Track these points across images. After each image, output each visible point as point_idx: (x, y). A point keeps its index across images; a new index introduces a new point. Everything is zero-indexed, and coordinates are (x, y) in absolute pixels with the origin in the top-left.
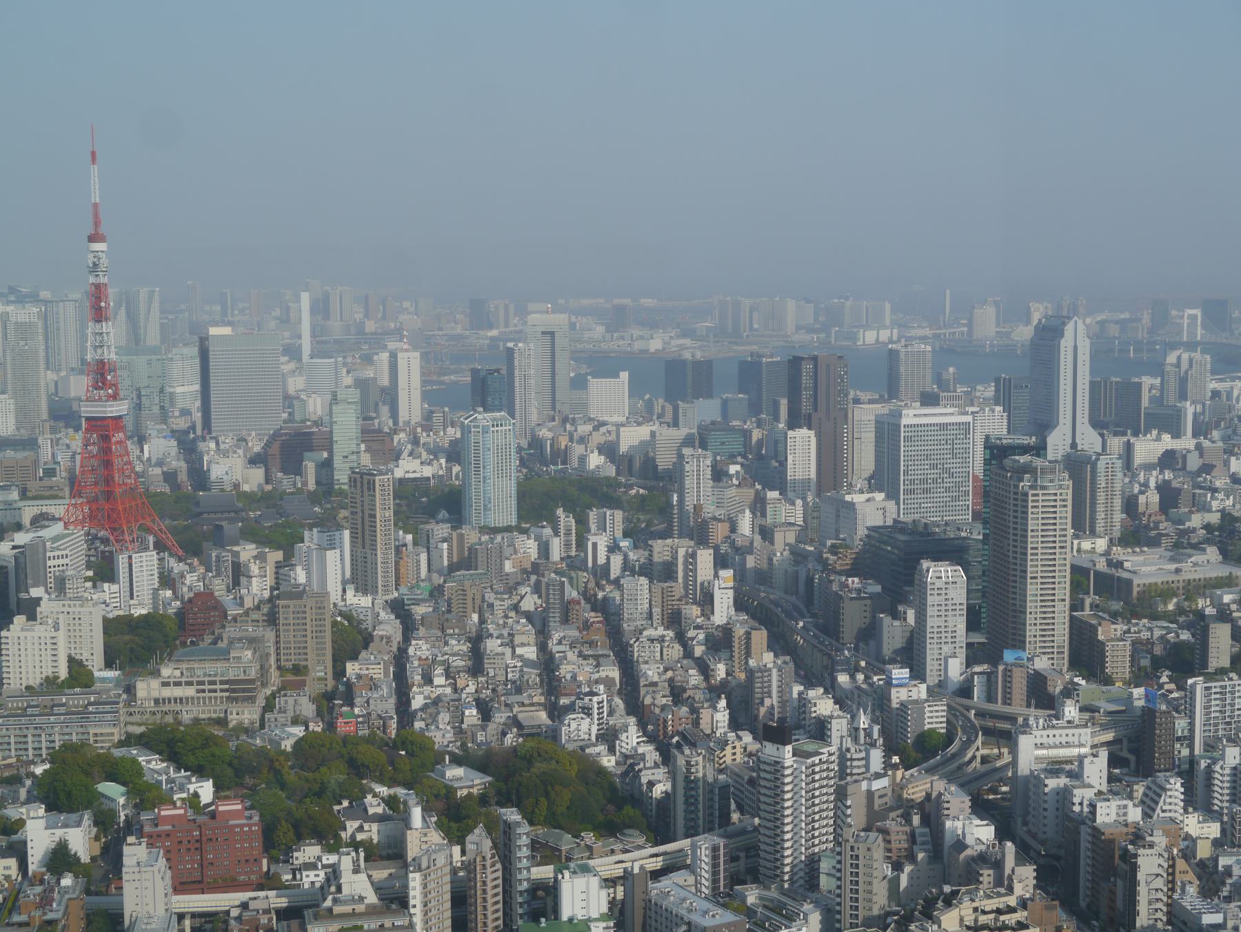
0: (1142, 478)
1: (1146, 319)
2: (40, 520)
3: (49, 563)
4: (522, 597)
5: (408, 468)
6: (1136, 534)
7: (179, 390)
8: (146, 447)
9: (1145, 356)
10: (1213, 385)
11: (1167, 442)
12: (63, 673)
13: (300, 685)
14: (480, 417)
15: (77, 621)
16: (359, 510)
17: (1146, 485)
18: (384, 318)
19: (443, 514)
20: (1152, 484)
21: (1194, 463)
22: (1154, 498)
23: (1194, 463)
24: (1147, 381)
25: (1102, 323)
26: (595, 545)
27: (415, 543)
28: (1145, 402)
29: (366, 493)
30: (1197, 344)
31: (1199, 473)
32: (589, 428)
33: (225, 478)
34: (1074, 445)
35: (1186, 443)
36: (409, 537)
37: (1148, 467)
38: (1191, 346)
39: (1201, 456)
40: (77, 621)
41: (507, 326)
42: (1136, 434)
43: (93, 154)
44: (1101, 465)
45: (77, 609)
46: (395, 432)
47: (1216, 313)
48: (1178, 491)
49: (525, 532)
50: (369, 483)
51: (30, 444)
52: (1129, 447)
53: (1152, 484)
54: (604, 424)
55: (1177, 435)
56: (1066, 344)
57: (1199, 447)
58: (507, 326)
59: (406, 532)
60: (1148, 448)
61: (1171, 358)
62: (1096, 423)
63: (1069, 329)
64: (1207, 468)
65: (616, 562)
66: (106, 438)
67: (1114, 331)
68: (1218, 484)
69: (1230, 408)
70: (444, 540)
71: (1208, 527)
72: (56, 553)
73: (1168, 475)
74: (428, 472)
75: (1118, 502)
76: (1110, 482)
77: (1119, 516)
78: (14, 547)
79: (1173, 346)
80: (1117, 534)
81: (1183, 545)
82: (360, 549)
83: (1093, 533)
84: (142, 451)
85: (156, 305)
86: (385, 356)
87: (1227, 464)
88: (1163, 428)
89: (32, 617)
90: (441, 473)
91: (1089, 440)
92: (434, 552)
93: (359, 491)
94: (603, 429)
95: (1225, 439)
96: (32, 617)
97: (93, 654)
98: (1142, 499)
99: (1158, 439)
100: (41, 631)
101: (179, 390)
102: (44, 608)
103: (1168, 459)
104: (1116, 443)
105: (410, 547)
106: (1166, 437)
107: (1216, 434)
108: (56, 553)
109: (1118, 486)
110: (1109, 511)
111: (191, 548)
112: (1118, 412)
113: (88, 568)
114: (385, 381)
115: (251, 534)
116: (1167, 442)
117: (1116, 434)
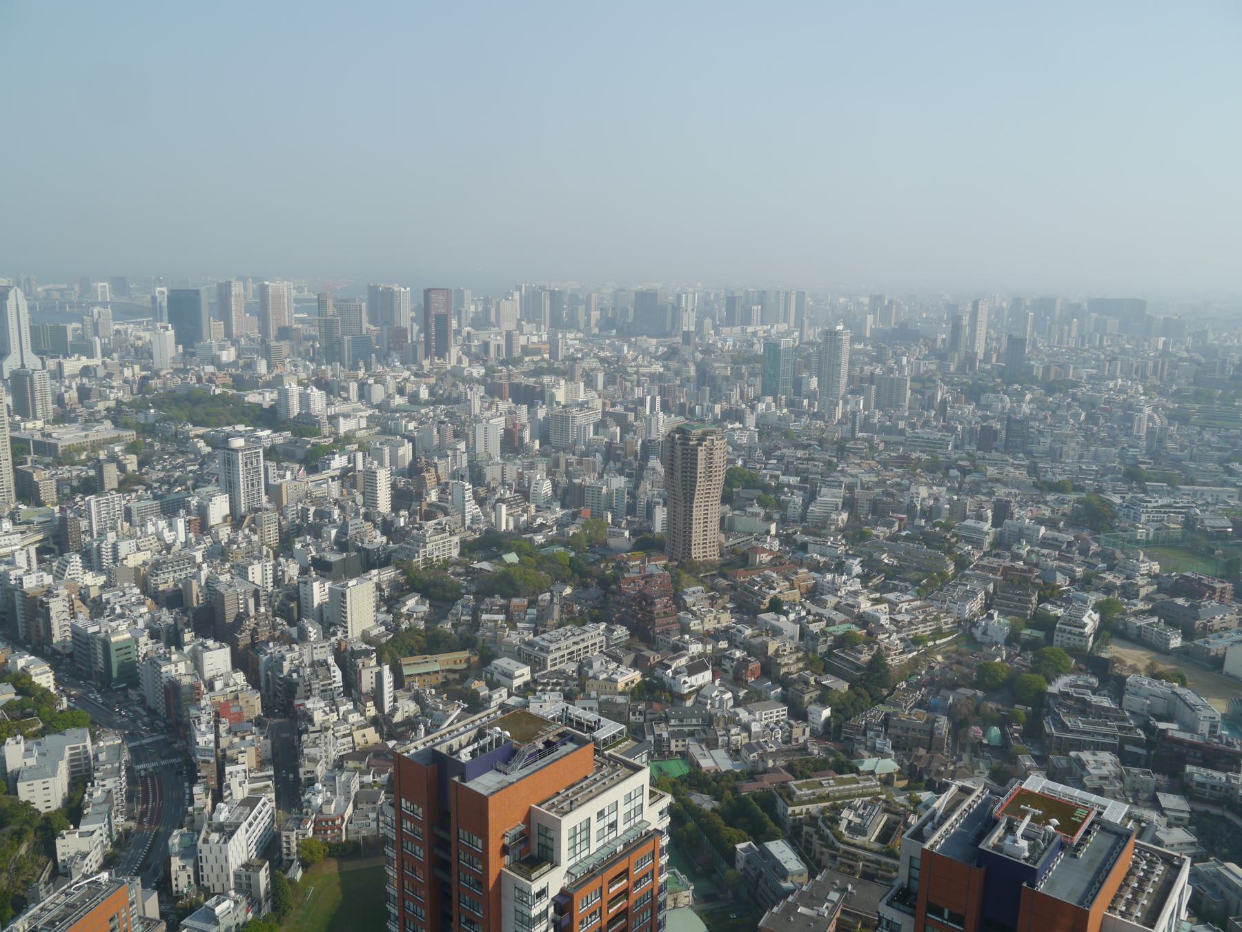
0: (67, 382)
1: (77, 288)
6: (63, 416)
9: (76, 311)
10: (117, 327)
11: (85, 361)
17: (70, 387)
20: (74, 386)
21: (101, 372)
22: (76, 395)
23: (101, 372)
24: (72, 327)
25: (47, 291)
28: (70, 338)
30: (107, 303)
31: (104, 379)
34: (23, 366)
35: (97, 361)
37: (73, 377)
38: (104, 304)
39: (106, 367)
42: (65, 357)
44: (36, 377)
47: (119, 285)
48: (90, 390)
52: (60, 365)
53: (74, 386)
55: (91, 356)
56: (11, 303)
57: (104, 363)
60: (72, 365)
61: (96, 310)
62: (38, 351)
63: (12, 294)
64: (110, 375)
67: (56, 295)
68: (114, 384)
69: (126, 340)
71: (108, 409)
73: (85, 380)
75: (49, 398)
76: (43, 387)
77: (51, 407)
79: (94, 305)
80: (51, 417)
81: (92, 420)
83: (35, 418)
87: (122, 372)
88: (82, 353)
91: (33, 361)
95: (121, 358)
98: (66, 396)
99: (79, 359)
103: (86, 371)
104: (51, 364)
106: (84, 358)
107: (115, 355)
109: (49, 389)
110: (44, 403)
112: (51, 342)
116: (85, 361)
117: (52, 358)
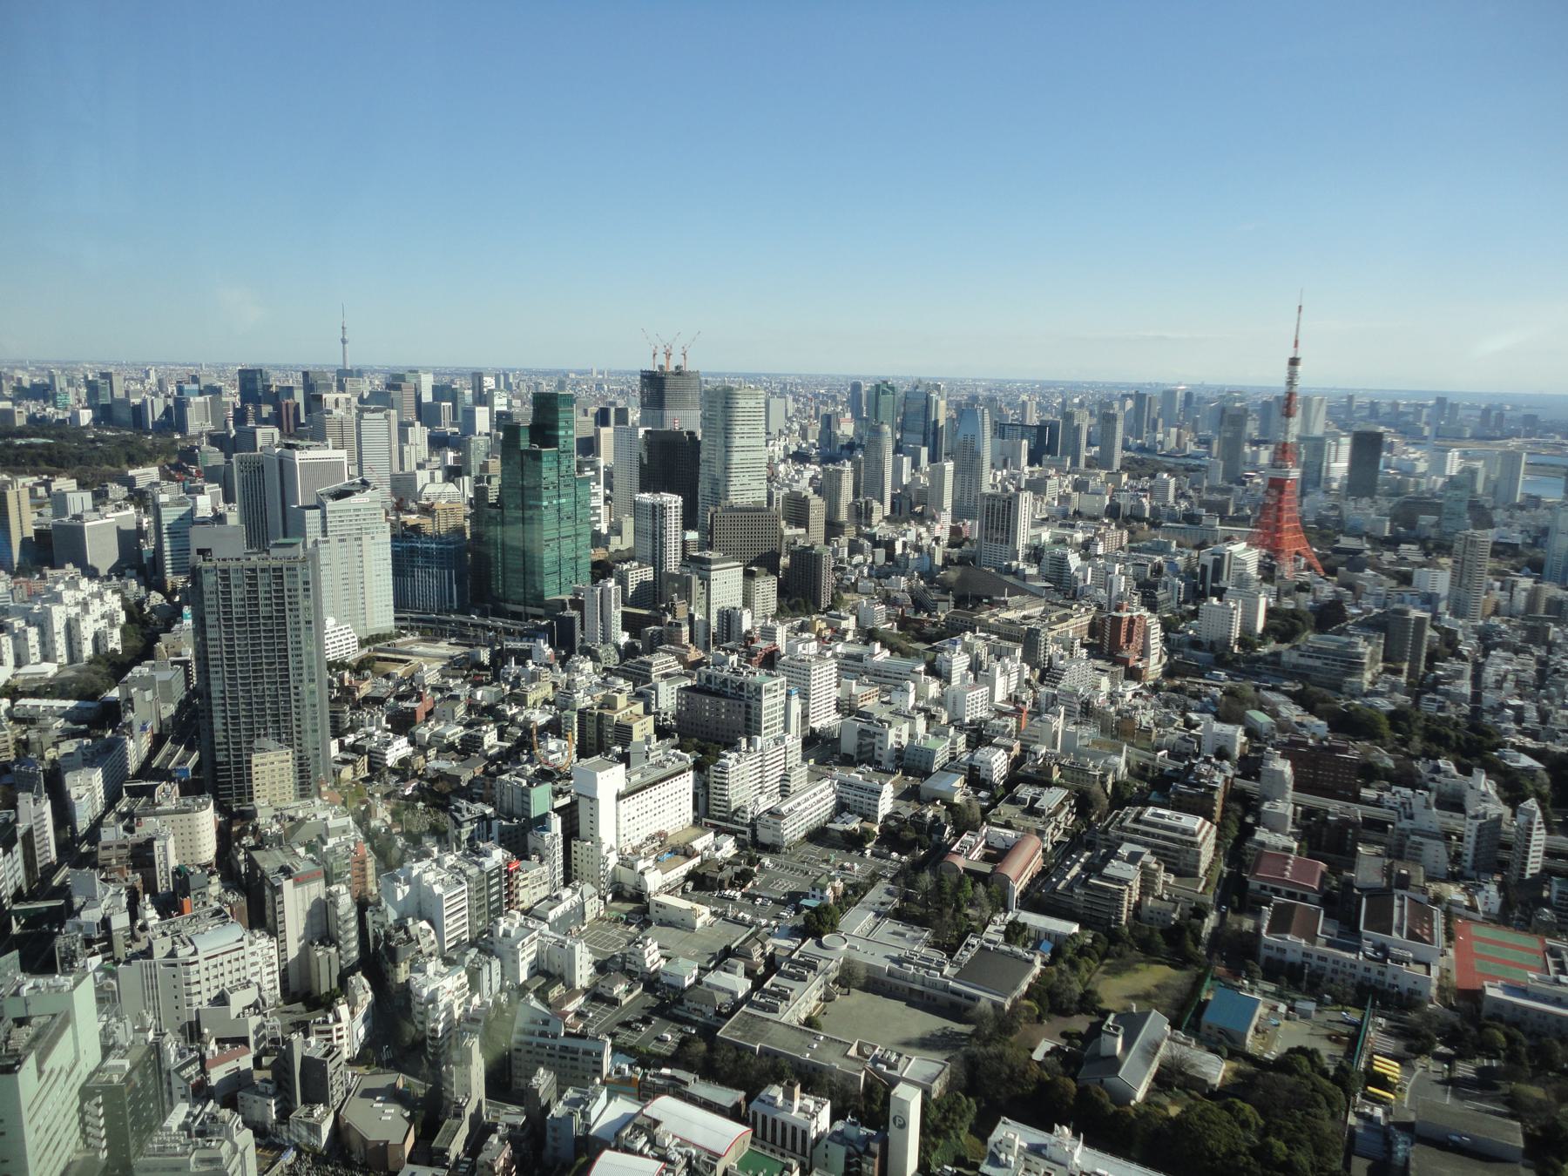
2: (1228, 539)
13: (1398, 672)
27: (1502, 589)
36: (1498, 584)
46: (1494, 508)
66: (1282, 492)
74: (1516, 538)
85: (1323, 409)
96: (1220, 599)
111: (1331, 571)
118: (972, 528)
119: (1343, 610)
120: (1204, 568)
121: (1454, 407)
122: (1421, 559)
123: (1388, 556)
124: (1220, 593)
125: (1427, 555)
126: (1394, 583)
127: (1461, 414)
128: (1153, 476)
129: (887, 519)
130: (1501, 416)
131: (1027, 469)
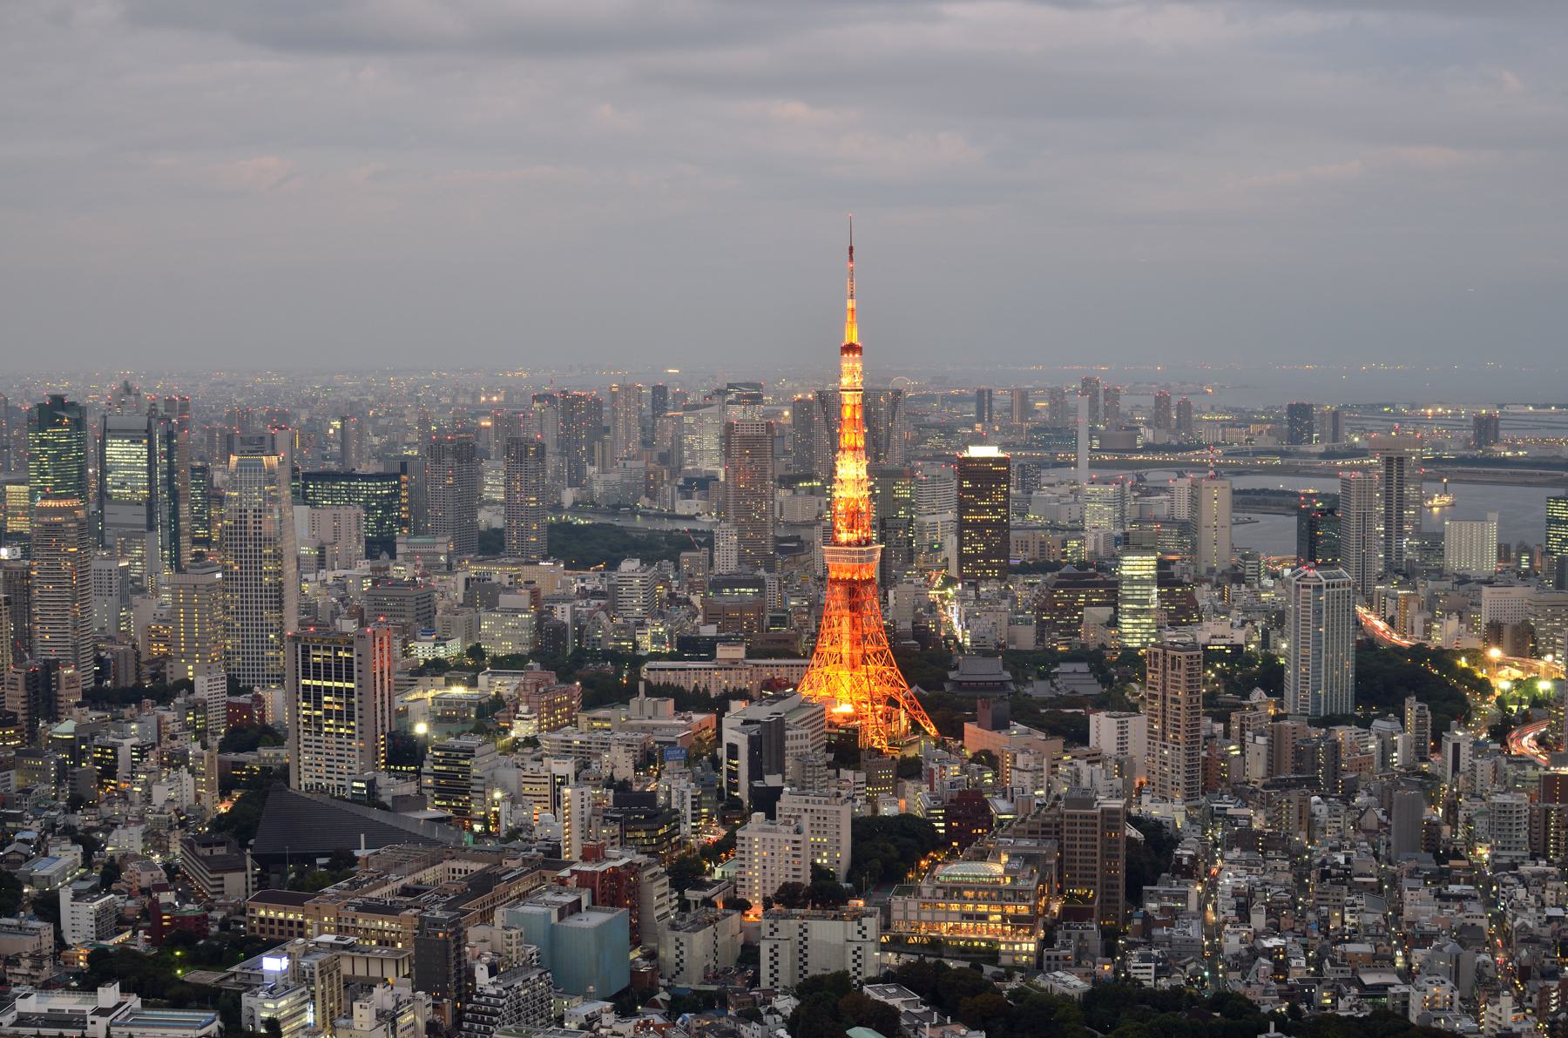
3: (787, 744)
4: (1362, 814)
5: (1216, 632)
7: (929, 519)
8: (891, 593)
12: (806, 878)
14: (1312, 573)
15: (822, 822)
16: (1160, 694)
18: (1179, 427)
19: (1258, 695)
26: (1456, 747)
27: (1227, 734)
29: (1169, 671)
32: (1448, 584)
33: (988, 636)
40: (822, 822)
41: (1335, 439)
43: (851, 249)
45: (823, 807)
46: (1199, 581)
49: (1365, 723)
50: (1174, 658)
51: (759, 583)
54: (1463, 580)
58: (1335, 439)
59: (1217, 719)
65: (1485, 766)
70: (1262, 735)
72: (794, 732)
78: (746, 722)
82: (1158, 742)
84: (886, 594)
86: (1185, 483)
89: (771, 815)
90: (1255, 638)
92: (1250, 748)
93: (1160, 670)
94: (1463, 588)
96: (771, 815)
97: (837, 854)
100: (785, 833)
101: (929, 519)
102: (786, 803)
105: (1220, 739)
108: (794, 732)
113: (829, 748)
114: (1183, 513)
115: (1026, 712)
118: (276, 703)
119: (985, 805)
120: (733, 751)
121: (1112, 395)
122: (1096, 689)
123: (1038, 689)
124: (766, 801)
125: (1106, 680)
126: (1059, 742)
127: (1125, 403)
128: (613, 565)
129: (93, 698)
130: (1184, 408)
131: (364, 566)
